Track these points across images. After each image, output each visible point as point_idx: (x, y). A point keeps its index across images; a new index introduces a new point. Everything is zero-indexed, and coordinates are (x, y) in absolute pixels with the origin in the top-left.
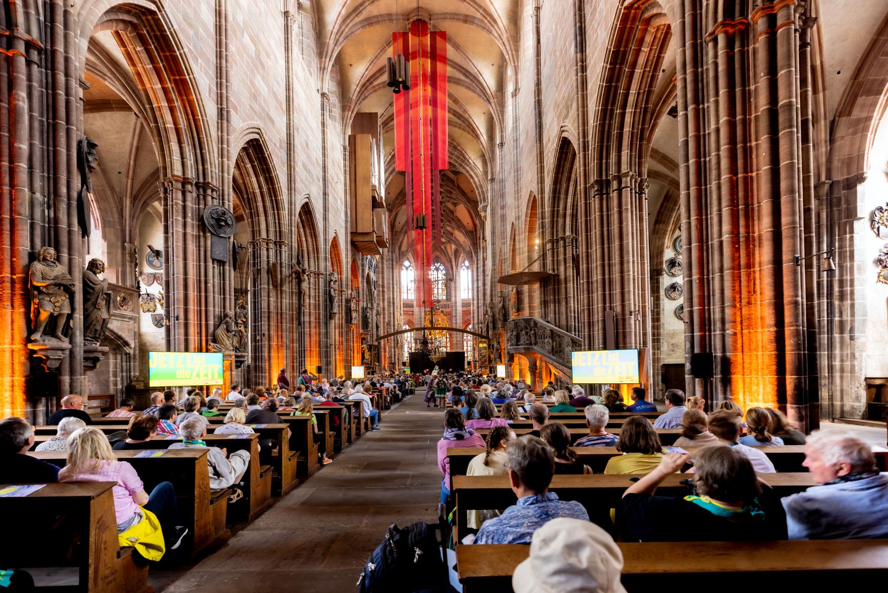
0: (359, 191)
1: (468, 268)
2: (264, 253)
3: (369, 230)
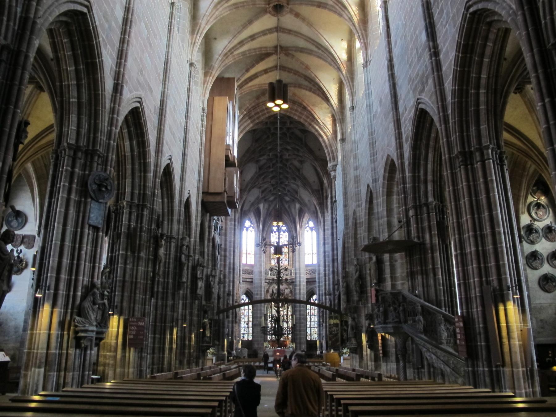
1: (312, 229)
2: (125, 216)
3: (220, 189)
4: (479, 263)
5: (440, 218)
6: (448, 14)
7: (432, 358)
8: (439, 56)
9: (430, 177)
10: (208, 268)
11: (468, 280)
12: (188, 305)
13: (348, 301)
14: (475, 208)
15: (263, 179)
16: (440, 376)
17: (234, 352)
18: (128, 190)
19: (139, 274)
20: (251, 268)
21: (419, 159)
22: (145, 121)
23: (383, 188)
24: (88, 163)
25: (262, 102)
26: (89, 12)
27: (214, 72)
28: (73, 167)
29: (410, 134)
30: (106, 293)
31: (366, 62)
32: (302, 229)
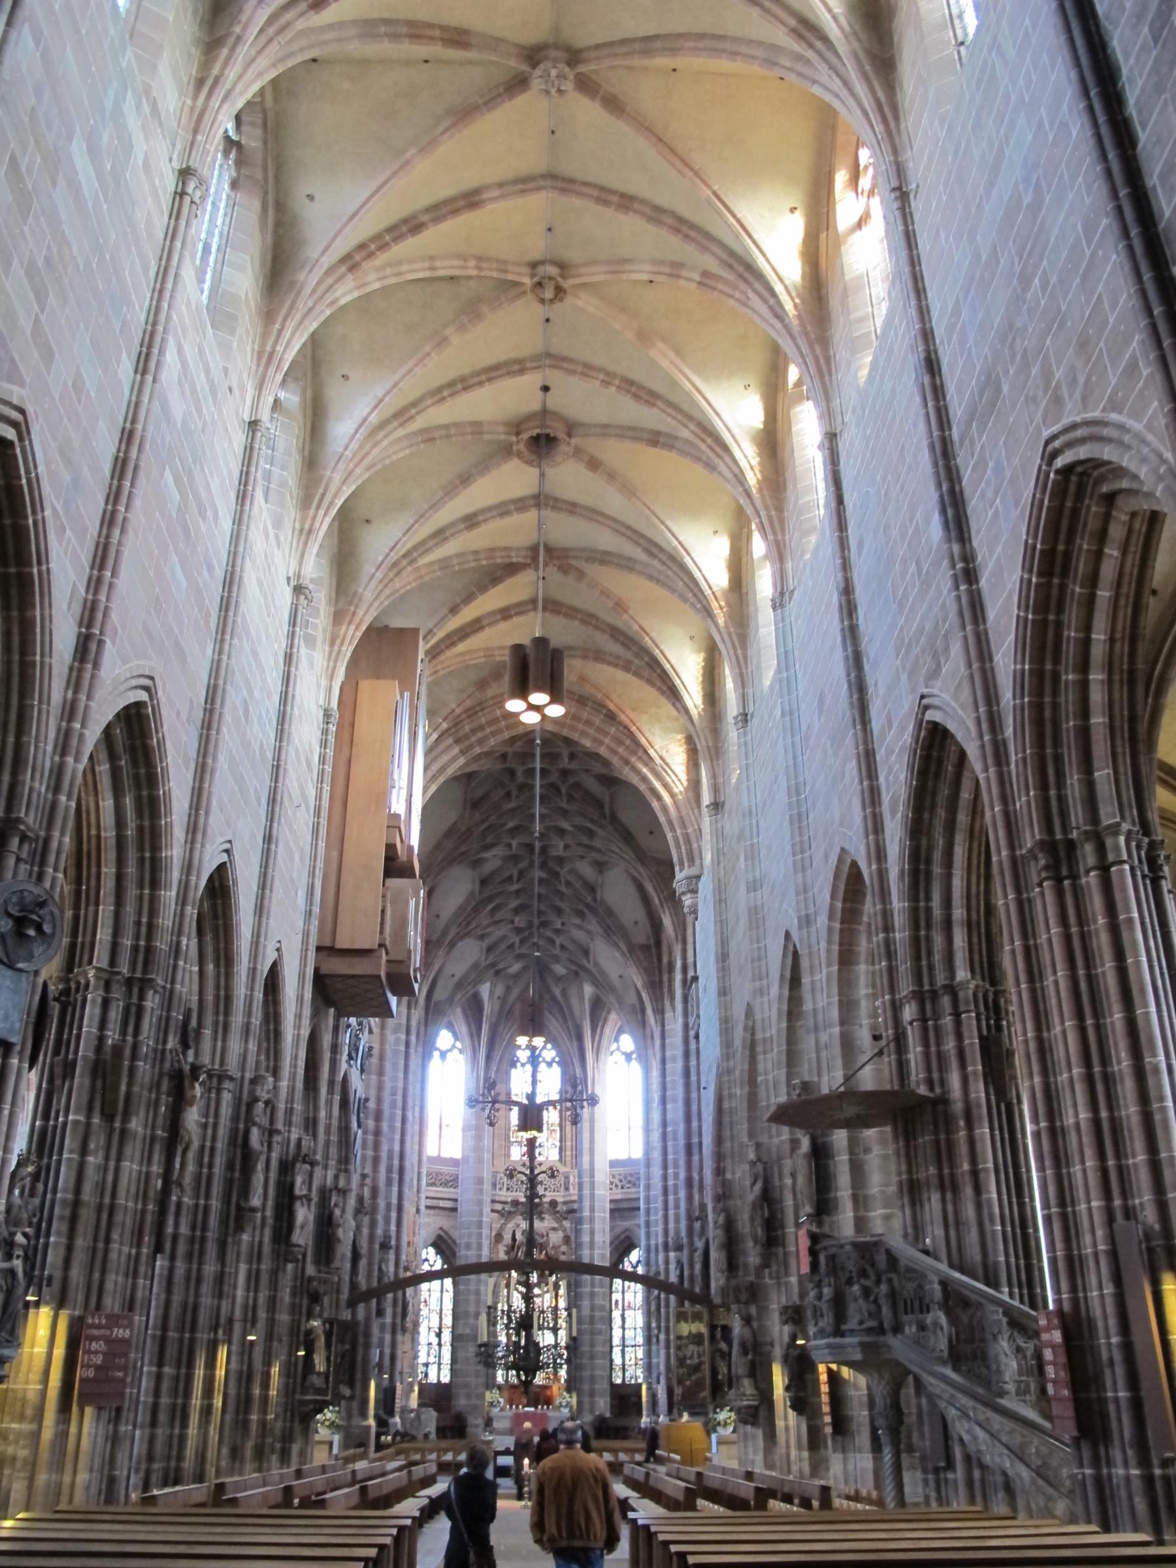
0: (352, 831)
1: (628, 1057)
2: (91, 1012)
4: (1101, 1156)
5: (988, 1026)
6: (998, 468)
7: (975, 1438)
8: (977, 582)
9: (958, 913)
10: (326, 1167)
11: (1073, 1205)
12: (264, 1279)
13: (732, 1265)
15: (493, 911)
16: (1001, 1494)
17: (397, 1419)
18: (103, 935)
20: (452, 1170)
21: (929, 861)
22: (161, 743)
23: (829, 942)
25: (492, 698)
26: (21, 439)
27: (361, 613)
30: (19, 1238)
31: (782, 594)
32: (602, 1056)
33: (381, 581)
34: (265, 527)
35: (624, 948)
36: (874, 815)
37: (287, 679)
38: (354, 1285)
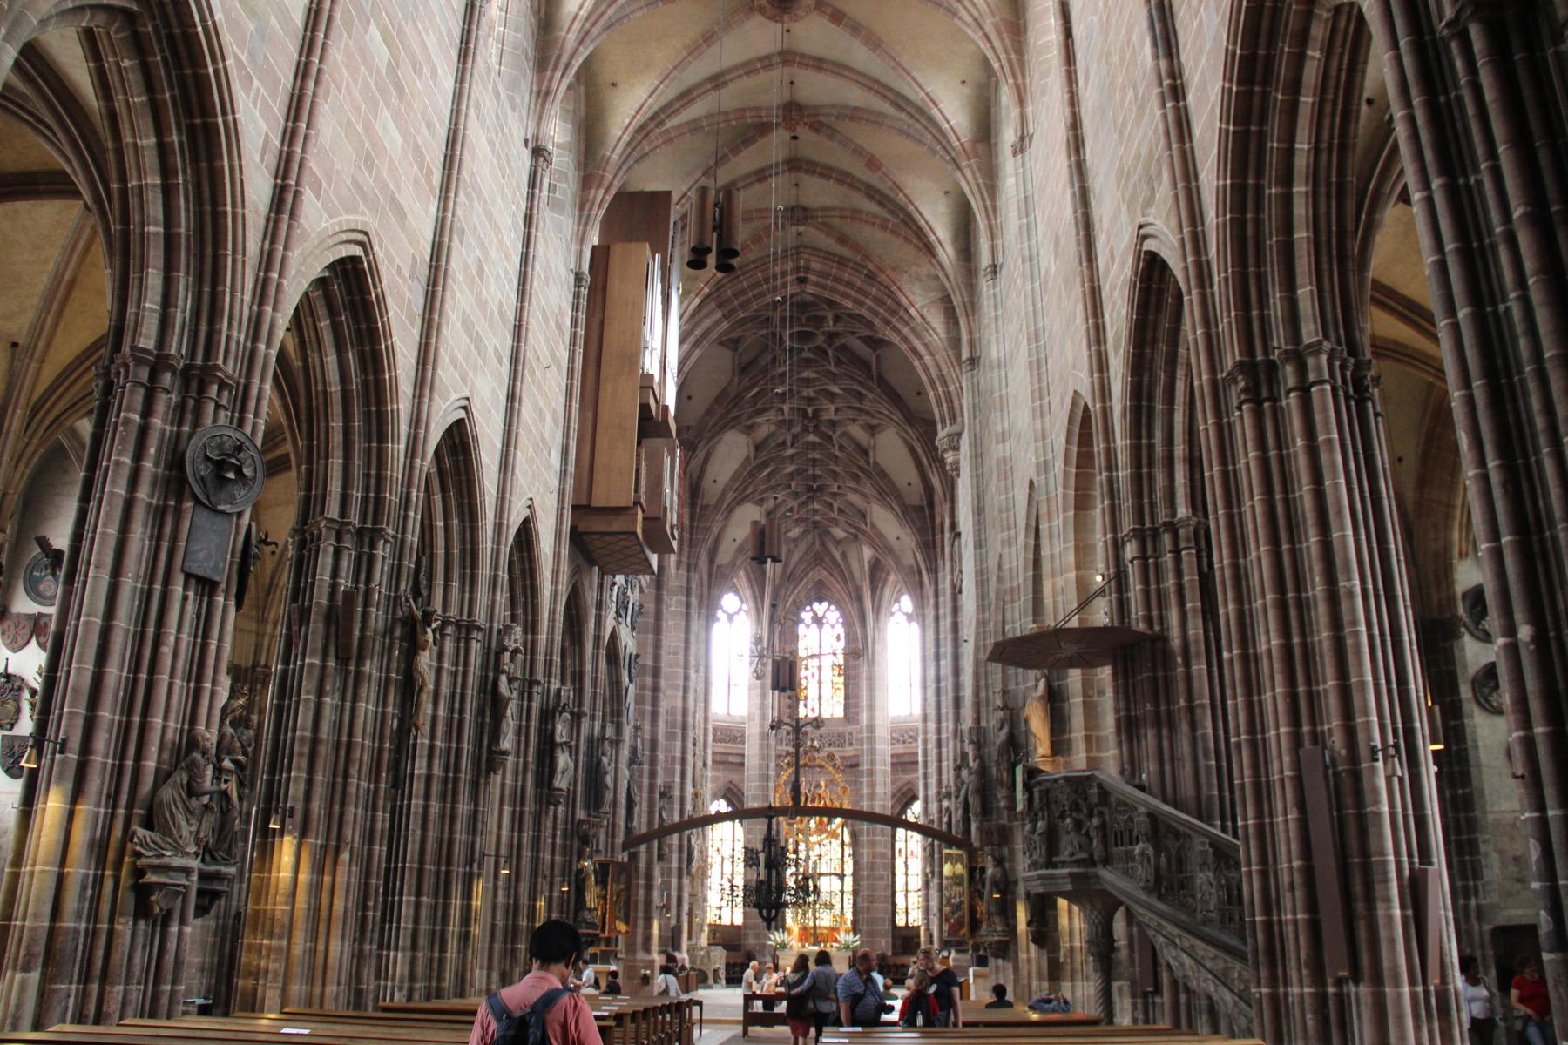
1: (909, 617)
2: (326, 560)
3: (625, 500)
4: (1291, 681)
7: (1182, 965)
8: (1184, 99)
10: (593, 718)
11: (1263, 732)
12: (528, 821)
14: (1281, 522)
18: (335, 488)
19: (360, 721)
21: (1151, 398)
22: (381, 298)
23: (1065, 487)
24: (191, 402)
28: (147, 412)
29: (1124, 332)
31: (1022, 139)
32: (882, 616)
33: (629, 144)
34: (495, 87)
35: (898, 509)
36: (1099, 353)
37: (527, 240)
38: (629, 830)
